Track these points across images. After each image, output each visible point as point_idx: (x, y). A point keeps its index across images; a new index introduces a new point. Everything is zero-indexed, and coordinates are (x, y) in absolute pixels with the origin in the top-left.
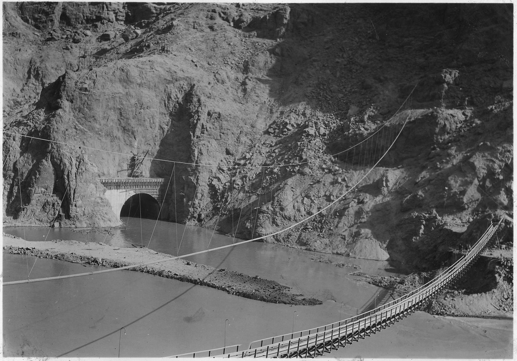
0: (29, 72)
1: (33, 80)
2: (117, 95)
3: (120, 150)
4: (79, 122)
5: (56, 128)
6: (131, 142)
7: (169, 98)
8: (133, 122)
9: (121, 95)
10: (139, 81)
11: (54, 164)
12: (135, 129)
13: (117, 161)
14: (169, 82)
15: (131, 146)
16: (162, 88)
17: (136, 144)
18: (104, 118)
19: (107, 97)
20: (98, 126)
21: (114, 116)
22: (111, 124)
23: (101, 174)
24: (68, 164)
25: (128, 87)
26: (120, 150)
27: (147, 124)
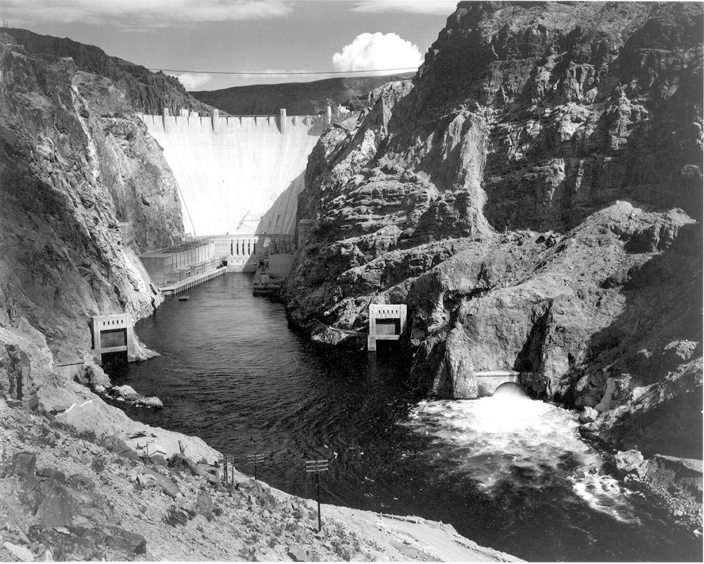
0: (481, 273)
1: (482, 280)
7: (534, 314)
8: (505, 333)
10: (510, 305)
14: (535, 303)
15: (505, 349)
16: (530, 307)
17: (509, 347)
21: (492, 330)
26: (497, 352)
27: (517, 333)
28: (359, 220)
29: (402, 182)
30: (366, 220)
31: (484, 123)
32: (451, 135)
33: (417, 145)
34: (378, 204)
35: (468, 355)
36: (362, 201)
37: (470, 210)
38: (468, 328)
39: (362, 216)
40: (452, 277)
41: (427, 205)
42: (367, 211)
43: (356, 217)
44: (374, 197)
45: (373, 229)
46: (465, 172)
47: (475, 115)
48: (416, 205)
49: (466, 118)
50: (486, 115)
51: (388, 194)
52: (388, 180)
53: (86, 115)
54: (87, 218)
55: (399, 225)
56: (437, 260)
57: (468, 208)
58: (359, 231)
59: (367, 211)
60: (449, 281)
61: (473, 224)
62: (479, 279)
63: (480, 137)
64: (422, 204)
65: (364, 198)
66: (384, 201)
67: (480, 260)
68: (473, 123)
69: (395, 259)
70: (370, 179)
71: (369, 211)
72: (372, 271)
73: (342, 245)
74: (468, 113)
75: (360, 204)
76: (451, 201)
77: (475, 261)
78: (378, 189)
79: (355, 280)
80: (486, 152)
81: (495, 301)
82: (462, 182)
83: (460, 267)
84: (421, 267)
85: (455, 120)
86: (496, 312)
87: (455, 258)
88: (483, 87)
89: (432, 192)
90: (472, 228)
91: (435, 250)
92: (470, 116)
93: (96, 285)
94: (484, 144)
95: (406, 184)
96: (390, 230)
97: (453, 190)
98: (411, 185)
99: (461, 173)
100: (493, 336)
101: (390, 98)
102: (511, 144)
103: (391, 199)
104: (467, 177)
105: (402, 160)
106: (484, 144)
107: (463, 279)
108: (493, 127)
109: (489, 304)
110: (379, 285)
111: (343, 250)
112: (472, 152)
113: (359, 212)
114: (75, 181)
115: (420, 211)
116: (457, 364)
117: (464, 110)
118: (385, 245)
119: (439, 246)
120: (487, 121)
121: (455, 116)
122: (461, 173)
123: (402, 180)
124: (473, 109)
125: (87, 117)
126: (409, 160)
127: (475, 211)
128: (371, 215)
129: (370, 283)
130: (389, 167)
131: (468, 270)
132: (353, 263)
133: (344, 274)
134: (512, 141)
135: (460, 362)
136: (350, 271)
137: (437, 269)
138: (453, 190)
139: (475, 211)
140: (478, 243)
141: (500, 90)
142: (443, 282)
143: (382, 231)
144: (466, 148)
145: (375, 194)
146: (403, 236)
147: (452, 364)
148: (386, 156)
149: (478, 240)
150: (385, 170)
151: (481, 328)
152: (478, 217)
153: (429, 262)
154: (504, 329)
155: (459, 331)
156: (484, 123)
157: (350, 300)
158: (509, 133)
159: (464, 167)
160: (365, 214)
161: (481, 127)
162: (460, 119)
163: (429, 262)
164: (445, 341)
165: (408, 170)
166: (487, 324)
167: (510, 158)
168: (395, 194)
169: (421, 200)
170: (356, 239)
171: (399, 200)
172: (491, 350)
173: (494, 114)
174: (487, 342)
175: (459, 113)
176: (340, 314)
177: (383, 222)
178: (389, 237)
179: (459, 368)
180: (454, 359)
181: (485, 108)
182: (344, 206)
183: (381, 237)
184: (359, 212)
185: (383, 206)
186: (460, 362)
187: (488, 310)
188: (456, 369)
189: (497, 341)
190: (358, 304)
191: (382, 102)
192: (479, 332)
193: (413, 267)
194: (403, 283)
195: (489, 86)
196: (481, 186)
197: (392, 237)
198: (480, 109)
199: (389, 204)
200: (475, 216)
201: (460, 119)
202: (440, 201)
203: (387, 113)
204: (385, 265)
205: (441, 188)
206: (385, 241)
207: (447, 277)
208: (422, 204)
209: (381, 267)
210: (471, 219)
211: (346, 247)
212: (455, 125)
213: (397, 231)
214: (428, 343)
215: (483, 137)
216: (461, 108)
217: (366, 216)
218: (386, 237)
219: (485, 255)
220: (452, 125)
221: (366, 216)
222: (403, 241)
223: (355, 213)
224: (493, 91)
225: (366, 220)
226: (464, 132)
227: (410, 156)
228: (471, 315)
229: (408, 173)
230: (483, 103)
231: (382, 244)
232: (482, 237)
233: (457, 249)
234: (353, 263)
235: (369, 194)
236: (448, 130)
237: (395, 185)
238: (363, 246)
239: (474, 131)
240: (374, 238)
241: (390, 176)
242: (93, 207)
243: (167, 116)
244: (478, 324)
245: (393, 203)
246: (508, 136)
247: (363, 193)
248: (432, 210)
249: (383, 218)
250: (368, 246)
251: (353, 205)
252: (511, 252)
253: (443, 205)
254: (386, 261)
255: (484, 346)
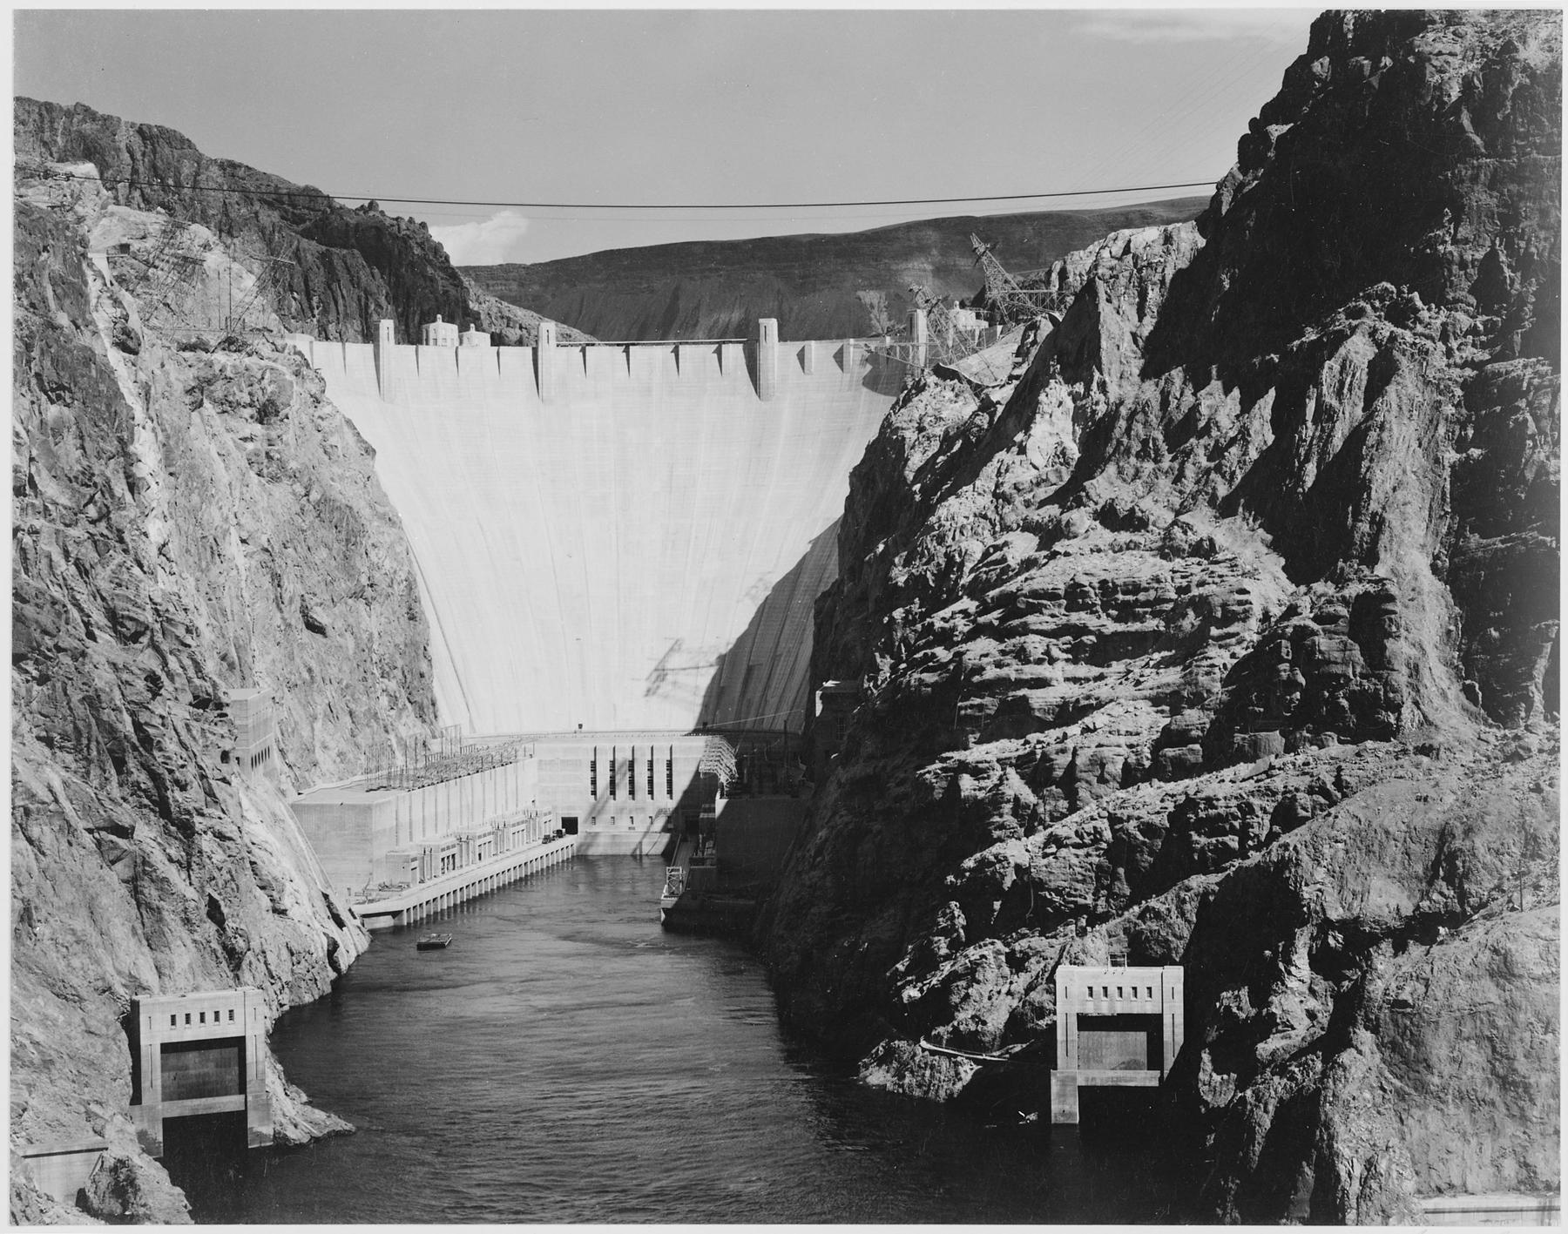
0: (1436, 864)
1: (1441, 885)
2: (1481, 1008)
3: (1495, 1130)
4: (1392, 1072)
5: (1330, 1093)
6: (1522, 1109)
8: (1522, 1065)
9: (1491, 1007)
10: (1538, 971)
11: (1317, 1170)
12: (1532, 1081)
13: (1488, 1152)
15: (1524, 1118)
18: (1454, 1060)
19: (1458, 1014)
20: (1436, 1080)
21: (1475, 1055)
22: (1469, 1073)
23: (1444, 1186)
24: (1343, 1175)
25: (1508, 986)
26: (1495, 1130)
28: (1020, 684)
29: (1164, 557)
30: (1041, 683)
31: (1438, 360)
32: (1331, 400)
33: (1214, 433)
34: (1084, 630)
35: (1394, 1141)
36: (1031, 619)
37: (1400, 649)
38: (1395, 1047)
39: (1030, 671)
40: (1338, 876)
41: (1251, 631)
42: (1047, 652)
43: (1011, 672)
44: (1069, 609)
45: (1068, 713)
46: (1378, 523)
47: (1408, 335)
48: (1214, 631)
49: (1378, 344)
50: (1444, 337)
51: (1119, 598)
52: (1117, 549)
53: (131, 344)
54: (125, 676)
55: (1156, 701)
56: (1287, 816)
57: (1389, 643)
58: (1016, 718)
59: (1047, 652)
60: (1328, 889)
61: (1406, 696)
62: (1430, 883)
63: (1426, 408)
64: (1232, 629)
65: (1038, 609)
66: (1104, 620)
67: (1435, 816)
68: (1404, 362)
69: (1142, 813)
70: (1057, 547)
71: (1055, 652)
72: (1063, 852)
73: (963, 767)
74: (1386, 329)
75: (1025, 630)
76: (1334, 618)
77: (1418, 821)
78: (1084, 580)
79: (1007, 883)
80: (1451, 456)
81: (1485, 957)
82: (1371, 557)
83: (1367, 843)
84: (1233, 842)
85: (1342, 351)
86: (1490, 992)
87: (1346, 813)
88: (1432, 243)
89: (1268, 586)
90: (1406, 712)
91: (1278, 783)
92: (1393, 338)
93: (151, 892)
94: (1442, 430)
95: (1178, 563)
96: (1126, 714)
97: (1340, 581)
98: (1195, 567)
99: (1364, 527)
100: (1479, 1075)
101: (1123, 281)
102: (1532, 427)
103: (1126, 613)
104: (1384, 539)
105: (1164, 483)
106: (1442, 430)
107: (1376, 883)
108: (1469, 372)
109: (1466, 965)
110: (1089, 901)
111: (967, 783)
112: (1400, 456)
113: (1022, 655)
114: (89, 554)
115: (1226, 654)
116: (1358, 1170)
117: (1369, 320)
118: (1109, 768)
119: (1290, 766)
120: (1449, 353)
121: (1341, 337)
122: (1364, 527)
123: (1167, 550)
124: (1401, 314)
125: (136, 353)
126: (1189, 485)
127: (1413, 652)
128: (1059, 665)
129: (1058, 891)
130: (1123, 507)
131: (1394, 850)
132: (1002, 827)
133: (969, 863)
134: (1537, 420)
135: (1370, 1164)
136: (989, 853)
137: (1286, 846)
138: (1340, 581)
139: (1413, 652)
140: (1425, 759)
141: (1492, 255)
142: (1307, 893)
143: (1098, 719)
144: (1380, 442)
145: (1075, 596)
146: (1170, 737)
147: (1342, 1170)
148: (1111, 469)
149: (1425, 750)
150: (1109, 517)
151: (1439, 1048)
152: (1425, 672)
153: (1261, 825)
154: (1518, 1051)
155: (1363, 1058)
156: (1438, 360)
157: (990, 951)
158: (1524, 394)
159: (1374, 506)
160: (1039, 662)
161: (1431, 374)
162: (1359, 350)
163: (1261, 825)
164: (1317, 1092)
165: (1183, 518)
166: (1459, 1034)
167: (1529, 475)
168: (1142, 597)
169: (1229, 618)
170: (1010, 747)
171: (1155, 615)
172: (1474, 1122)
173: (1473, 331)
174: (1461, 1097)
175: (1353, 330)
176: (955, 999)
177: (1102, 690)
178: (1123, 740)
179: (1364, 1183)
180: (1347, 1153)
181: (1444, 312)
182: (971, 636)
183: (1094, 739)
184: (1022, 655)
185: (1099, 635)
186: (1370, 1164)
187: (1462, 986)
188: (1354, 1189)
189: (1493, 1093)
190: (1017, 963)
191: (1095, 295)
192: (1434, 1060)
193: (1203, 840)
194: (1171, 895)
195: (1455, 242)
196: (1435, 569)
197: (1133, 740)
198: (1424, 315)
199: (1121, 627)
200: (1415, 670)
201: (1359, 350)
202: (1295, 621)
203: (1115, 329)
204: (1108, 835)
205: (1299, 573)
206: (1106, 752)
207: (1320, 874)
208: (1232, 629)
209: (1095, 841)
210: (1401, 678)
211: (977, 772)
212: (1343, 367)
213: (1150, 721)
214: (1258, 1099)
215: (1437, 406)
216: (1358, 313)
217: (1044, 671)
218: (1114, 739)
219: (1450, 799)
220: (1329, 371)
221: (1044, 671)
222: (1170, 752)
223: (1008, 659)
224: (1468, 257)
225: (1041, 683)
226: (1374, 390)
227: (1190, 471)
228: (1405, 1004)
229: (1186, 528)
230: (1436, 297)
231: (1099, 763)
232: (1438, 739)
233: (1353, 781)
234: (1002, 827)
235: (1052, 596)
236: (1318, 384)
237: (1142, 566)
238: (1036, 770)
239: (1406, 387)
240: (1070, 744)
241: (1124, 537)
242: (145, 640)
243: (549, 350)
244: (1428, 1033)
245: (1135, 627)
246: (1522, 403)
247: (1034, 594)
248: (1265, 653)
249: (1101, 677)
250: (1052, 769)
251: (999, 633)
252: (1537, 789)
253: (1302, 633)
254: (1113, 820)
255: (1451, 1109)
